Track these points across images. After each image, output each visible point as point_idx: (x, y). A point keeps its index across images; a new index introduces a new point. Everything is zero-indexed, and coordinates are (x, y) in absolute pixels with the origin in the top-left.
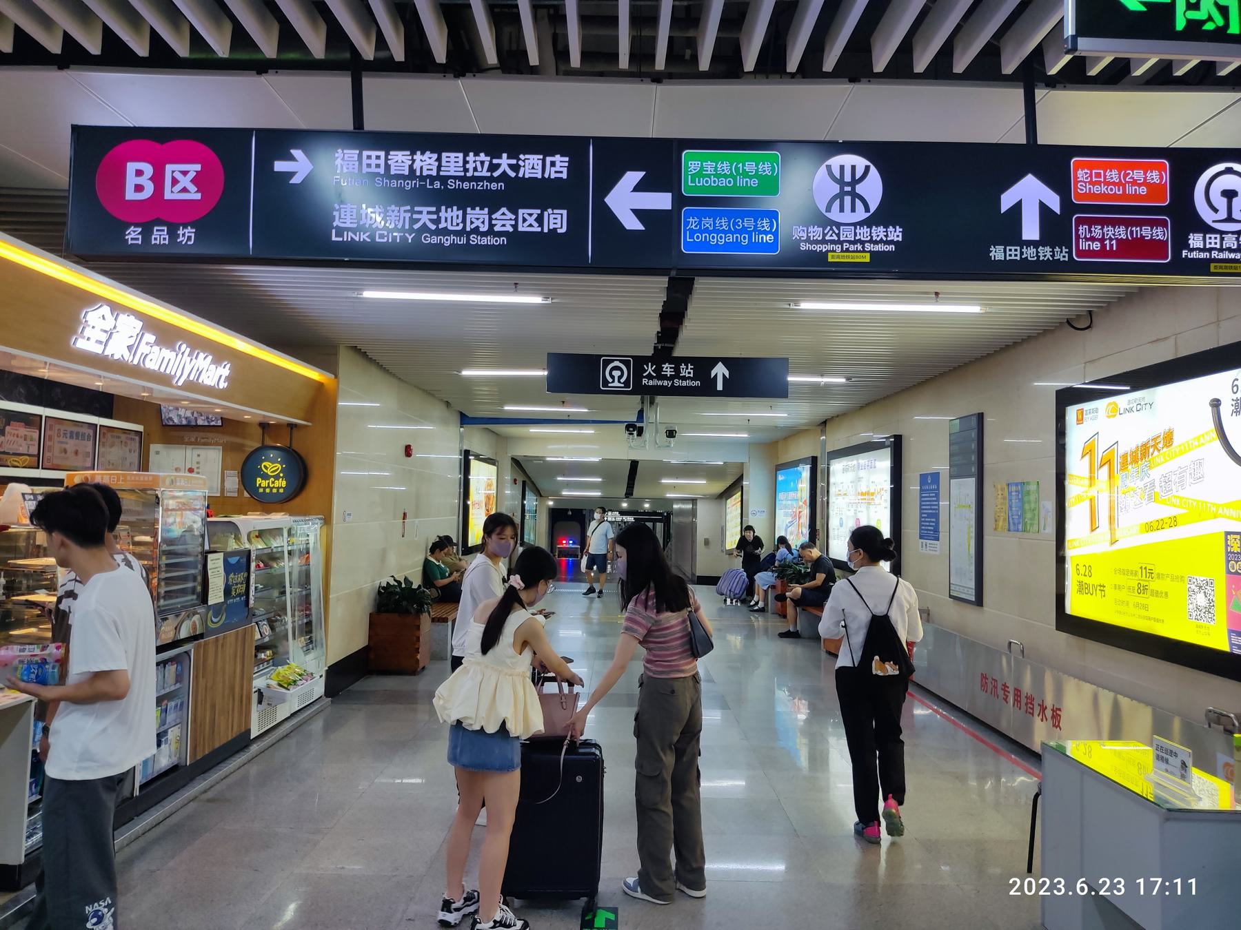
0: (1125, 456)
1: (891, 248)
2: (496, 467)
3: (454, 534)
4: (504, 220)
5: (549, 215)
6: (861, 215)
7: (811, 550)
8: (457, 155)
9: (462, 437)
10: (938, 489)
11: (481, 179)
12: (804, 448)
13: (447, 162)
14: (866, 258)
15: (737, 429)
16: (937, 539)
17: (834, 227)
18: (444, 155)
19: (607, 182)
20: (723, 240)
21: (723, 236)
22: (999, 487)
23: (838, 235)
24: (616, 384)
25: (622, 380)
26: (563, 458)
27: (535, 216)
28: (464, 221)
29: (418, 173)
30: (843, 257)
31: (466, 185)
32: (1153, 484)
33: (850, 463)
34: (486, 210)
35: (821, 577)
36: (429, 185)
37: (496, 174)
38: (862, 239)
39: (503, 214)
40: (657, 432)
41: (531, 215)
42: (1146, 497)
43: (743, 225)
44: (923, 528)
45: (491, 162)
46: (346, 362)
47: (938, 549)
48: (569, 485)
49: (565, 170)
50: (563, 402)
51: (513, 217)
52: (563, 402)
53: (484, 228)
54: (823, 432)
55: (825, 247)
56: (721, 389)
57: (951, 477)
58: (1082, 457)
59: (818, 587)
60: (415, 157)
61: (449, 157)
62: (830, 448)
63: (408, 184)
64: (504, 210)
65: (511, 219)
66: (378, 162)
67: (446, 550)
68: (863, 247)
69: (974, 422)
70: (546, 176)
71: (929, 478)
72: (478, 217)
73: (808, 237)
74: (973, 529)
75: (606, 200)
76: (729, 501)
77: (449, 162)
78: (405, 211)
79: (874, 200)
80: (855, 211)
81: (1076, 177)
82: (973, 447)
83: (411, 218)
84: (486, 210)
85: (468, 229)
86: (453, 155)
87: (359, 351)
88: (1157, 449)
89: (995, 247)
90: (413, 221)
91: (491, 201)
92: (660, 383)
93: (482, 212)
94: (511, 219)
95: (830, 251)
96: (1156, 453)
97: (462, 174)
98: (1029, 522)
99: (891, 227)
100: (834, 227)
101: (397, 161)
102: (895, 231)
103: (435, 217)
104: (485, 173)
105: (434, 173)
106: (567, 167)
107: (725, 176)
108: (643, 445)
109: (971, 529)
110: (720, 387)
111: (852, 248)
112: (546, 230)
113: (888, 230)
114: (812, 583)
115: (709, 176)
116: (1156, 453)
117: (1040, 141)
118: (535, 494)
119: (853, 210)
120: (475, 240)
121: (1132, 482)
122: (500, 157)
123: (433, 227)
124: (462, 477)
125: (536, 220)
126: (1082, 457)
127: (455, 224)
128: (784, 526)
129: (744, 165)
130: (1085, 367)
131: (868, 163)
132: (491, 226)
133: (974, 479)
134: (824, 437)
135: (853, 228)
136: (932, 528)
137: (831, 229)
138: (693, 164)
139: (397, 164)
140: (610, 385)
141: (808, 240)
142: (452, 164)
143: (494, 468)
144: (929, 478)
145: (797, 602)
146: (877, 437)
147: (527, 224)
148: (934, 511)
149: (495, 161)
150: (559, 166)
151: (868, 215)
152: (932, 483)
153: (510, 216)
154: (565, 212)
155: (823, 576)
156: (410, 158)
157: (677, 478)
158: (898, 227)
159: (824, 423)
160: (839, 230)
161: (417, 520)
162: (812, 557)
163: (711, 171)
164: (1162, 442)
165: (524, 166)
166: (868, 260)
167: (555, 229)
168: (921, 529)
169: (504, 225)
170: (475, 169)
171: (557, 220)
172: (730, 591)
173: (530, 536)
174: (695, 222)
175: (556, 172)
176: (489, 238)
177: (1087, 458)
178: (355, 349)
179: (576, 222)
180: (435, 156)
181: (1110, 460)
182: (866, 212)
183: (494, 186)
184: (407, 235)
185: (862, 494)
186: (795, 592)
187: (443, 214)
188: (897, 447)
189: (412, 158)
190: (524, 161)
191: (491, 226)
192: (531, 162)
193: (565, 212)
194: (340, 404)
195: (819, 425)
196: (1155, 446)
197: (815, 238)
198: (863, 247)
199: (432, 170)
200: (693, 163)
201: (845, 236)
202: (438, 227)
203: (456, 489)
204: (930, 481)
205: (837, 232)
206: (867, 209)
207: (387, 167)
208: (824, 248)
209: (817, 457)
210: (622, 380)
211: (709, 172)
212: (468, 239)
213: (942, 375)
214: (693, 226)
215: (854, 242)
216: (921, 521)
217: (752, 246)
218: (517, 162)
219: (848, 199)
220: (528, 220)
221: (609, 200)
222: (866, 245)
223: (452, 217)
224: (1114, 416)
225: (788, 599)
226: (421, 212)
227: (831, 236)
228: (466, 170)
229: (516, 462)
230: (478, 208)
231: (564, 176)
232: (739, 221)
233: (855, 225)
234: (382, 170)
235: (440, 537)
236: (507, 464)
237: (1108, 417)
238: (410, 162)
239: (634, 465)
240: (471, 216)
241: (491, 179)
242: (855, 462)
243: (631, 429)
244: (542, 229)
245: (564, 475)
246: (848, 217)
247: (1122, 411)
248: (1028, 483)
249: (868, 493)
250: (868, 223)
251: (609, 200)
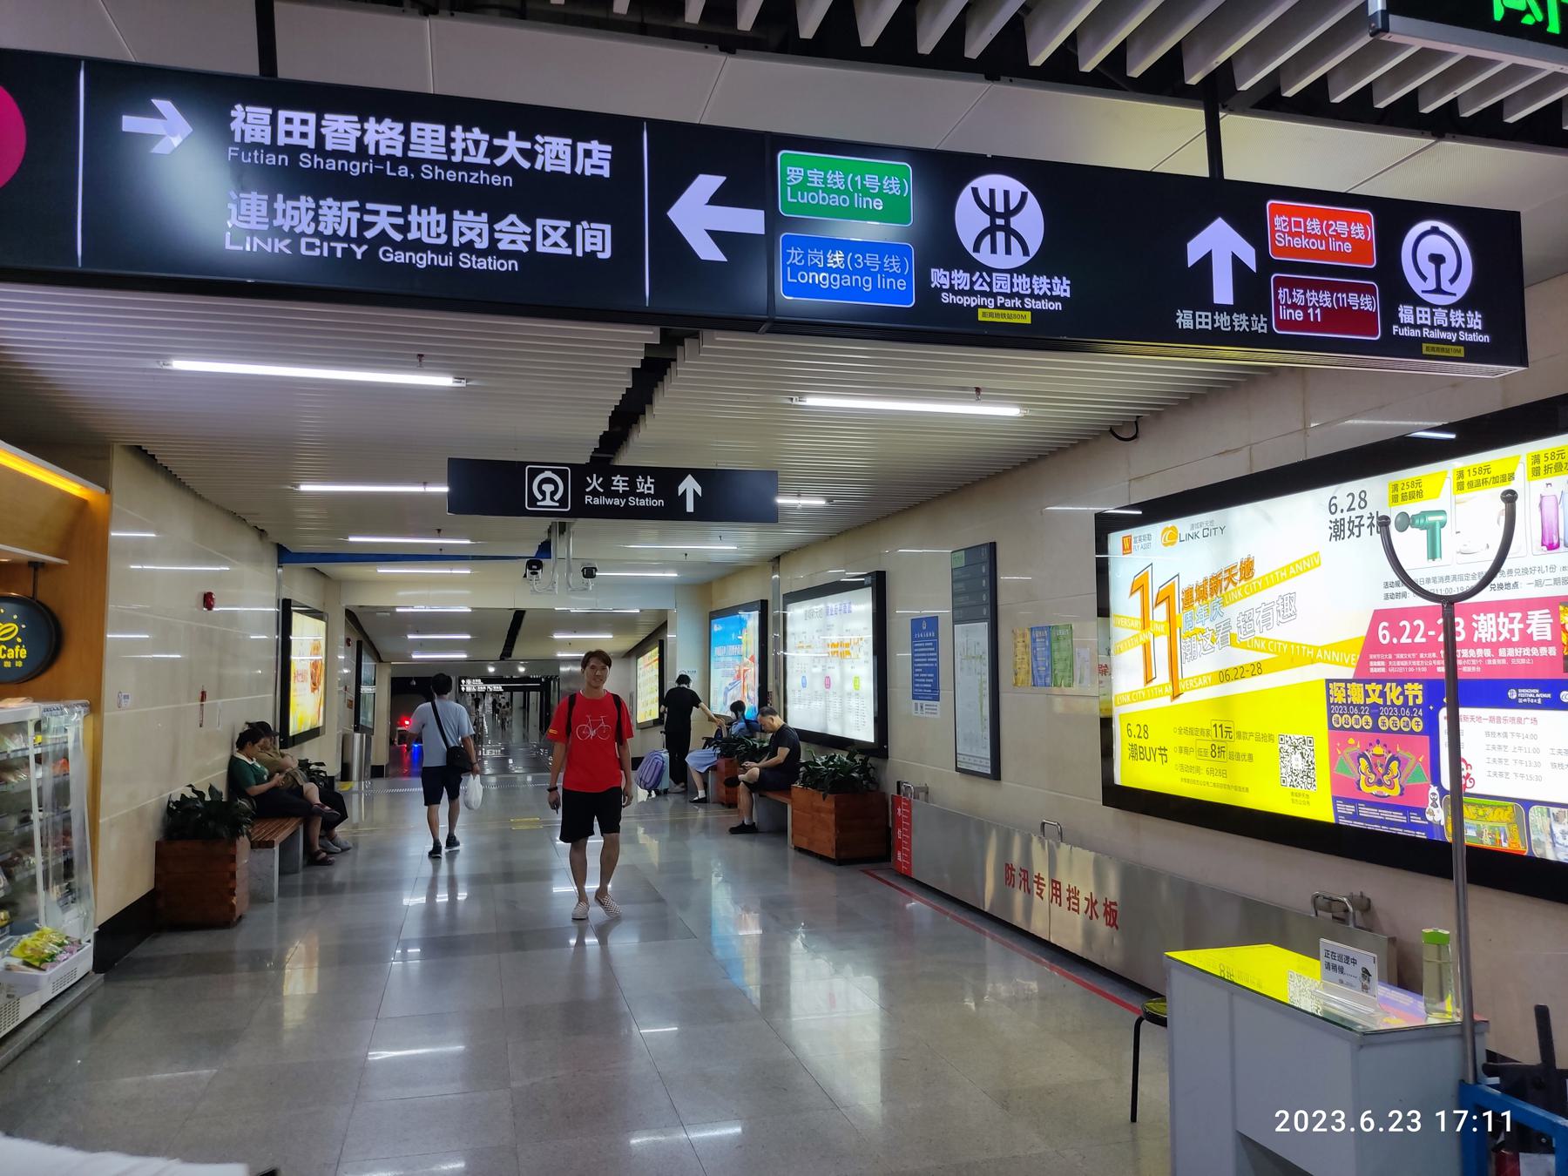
0: (1188, 592)
1: (1057, 306)
2: (324, 623)
3: (268, 716)
4: (513, 233)
5: (584, 230)
6: (1018, 259)
7: (773, 717)
9: (279, 581)
10: (937, 636)
11: (476, 167)
12: (750, 590)
13: (419, 137)
14: (1027, 319)
15: (664, 566)
16: (937, 699)
17: (984, 274)
18: (414, 126)
19: (671, 190)
20: (838, 283)
21: (838, 276)
22: (1019, 632)
23: (990, 285)
24: (548, 502)
25: (557, 497)
26: (413, 607)
27: (562, 231)
28: (449, 231)
29: (372, 151)
30: (997, 315)
31: (451, 175)
32: (1228, 624)
33: (815, 607)
34: (484, 216)
35: (783, 752)
36: (391, 171)
37: (499, 162)
38: (1021, 292)
39: (512, 224)
40: (570, 570)
41: (555, 228)
42: (1219, 639)
43: (865, 264)
44: (917, 685)
45: (490, 142)
46: (122, 469)
47: (938, 712)
48: (423, 646)
49: (606, 165)
50: (439, 530)
51: (528, 230)
52: (439, 530)
53: (482, 244)
54: (775, 569)
55: (974, 301)
56: (692, 511)
57: (955, 621)
58: (1132, 593)
59: (780, 765)
60: (366, 126)
61: (423, 130)
62: (785, 590)
63: (355, 166)
64: (513, 217)
65: (524, 233)
66: (304, 129)
67: (261, 742)
68: (1022, 303)
69: (985, 554)
70: (578, 170)
71: (924, 624)
72: (471, 226)
73: (952, 286)
74: (987, 685)
75: (668, 214)
76: (641, 660)
77: (423, 137)
78: (351, 209)
79: (1035, 242)
80: (1010, 254)
81: (1273, 226)
82: (984, 585)
83: (360, 221)
84: (484, 216)
85: (456, 244)
86: (429, 127)
87: (141, 453)
88: (1233, 582)
89: (1182, 312)
90: (363, 226)
91: (494, 204)
92: (609, 502)
93: (477, 218)
94: (524, 233)
95: (981, 307)
96: (1231, 587)
97: (445, 157)
98: (1060, 674)
99: (1056, 278)
100: (984, 274)
101: (336, 131)
102: (1062, 284)
103: (400, 221)
104: (481, 159)
105: (398, 153)
106: (611, 161)
107: (838, 192)
108: (550, 588)
109: (984, 686)
110: (690, 508)
111: (1008, 303)
112: (579, 253)
113: (1053, 281)
114: (773, 760)
115: (816, 190)
116: (1231, 587)
117: (1227, 176)
118: (374, 659)
119: (1008, 251)
120: (467, 261)
121: (1201, 619)
122: (506, 137)
123: (398, 237)
124: (280, 639)
125: (563, 237)
126: (1132, 593)
127: (433, 234)
128: (723, 690)
129: (863, 179)
130: (1129, 486)
131: (1025, 189)
132: (493, 241)
133: (986, 623)
134: (777, 576)
135: (1008, 276)
136: (930, 686)
137: (981, 276)
138: (792, 169)
139: (336, 135)
140: (539, 504)
141: (951, 290)
142: (428, 141)
143: (321, 624)
144: (924, 624)
145: (752, 787)
146: (849, 575)
147: (549, 242)
148: (932, 665)
149: (497, 142)
150: (597, 159)
151: (1027, 259)
152: (928, 630)
153: (523, 227)
154: (607, 228)
155: (787, 750)
156: (358, 126)
157: (575, 632)
158: (1064, 278)
159: (778, 558)
160: (991, 277)
161: (219, 701)
162: (772, 726)
163: (818, 183)
164: (1239, 574)
165: (543, 154)
166: (1028, 321)
167: (594, 253)
168: (914, 687)
169: (513, 242)
170: (465, 152)
171: (596, 239)
172: (641, 779)
173: (367, 717)
174: (799, 254)
175: (593, 166)
176: (490, 260)
177: (1138, 595)
178: (139, 452)
179: (625, 242)
180: (400, 127)
181: (1169, 597)
182: (1024, 255)
183: (496, 180)
184: (354, 247)
185: (833, 645)
186: (752, 774)
187: (413, 218)
188: (879, 584)
189: (362, 127)
190: (543, 145)
191: (493, 241)
192: (554, 147)
193: (607, 228)
194: (113, 534)
195: (772, 561)
196: (1230, 579)
197: (960, 288)
198: (1022, 303)
199: (394, 147)
200: (793, 169)
201: (998, 286)
202: (405, 237)
203: (271, 656)
204: (925, 628)
205: (989, 280)
206: (1026, 252)
207: (320, 138)
208: (972, 302)
209: (767, 601)
210: (557, 497)
211: (816, 185)
212: (456, 260)
213: (942, 497)
214: (796, 261)
215: (1011, 296)
216: (914, 678)
217: (877, 293)
218: (532, 146)
219: (1000, 236)
220: (551, 237)
221: (676, 214)
222: (1026, 300)
223: (429, 223)
224: (1173, 544)
225: (742, 783)
226: (376, 213)
227: (981, 285)
228: (450, 152)
229: (351, 615)
230: (470, 213)
231: (606, 173)
232: (859, 258)
233: (1011, 271)
234: (310, 143)
235: (250, 724)
236: (340, 619)
237: (1165, 545)
238: (359, 134)
239: (519, 615)
240: (462, 224)
241: (491, 169)
242: (822, 606)
243: (534, 567)
244: (574, 251)
245: (417, 632)
246: (999, 260)
247: (1183, 538)
248: (1057, 627)
249: (841, 644)
250: (1027, 270)
251: (676, 214)
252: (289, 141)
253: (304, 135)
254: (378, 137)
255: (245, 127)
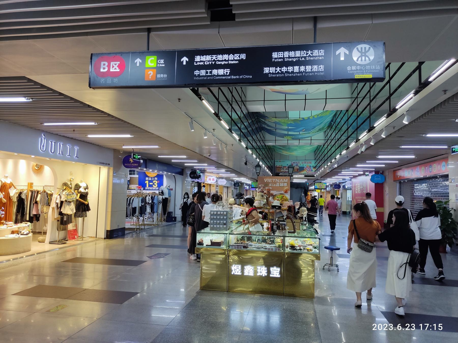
8: (299, 51)
29: (290, 57)
37: (308, 55)
45: (306, 52)
63: (294, 59)
86: (298, 51)
97: (300, 56)
122: (309, 51)
142: (298, 54)
149: (307, 52)
156: (289, 53)
170: (303, 55)
180: (294, 52)
228: (301, 55)
238: (289, 54)
252: (280, 57)
253: (280, 56)
254: (291, 54)
255: (274, 56)
